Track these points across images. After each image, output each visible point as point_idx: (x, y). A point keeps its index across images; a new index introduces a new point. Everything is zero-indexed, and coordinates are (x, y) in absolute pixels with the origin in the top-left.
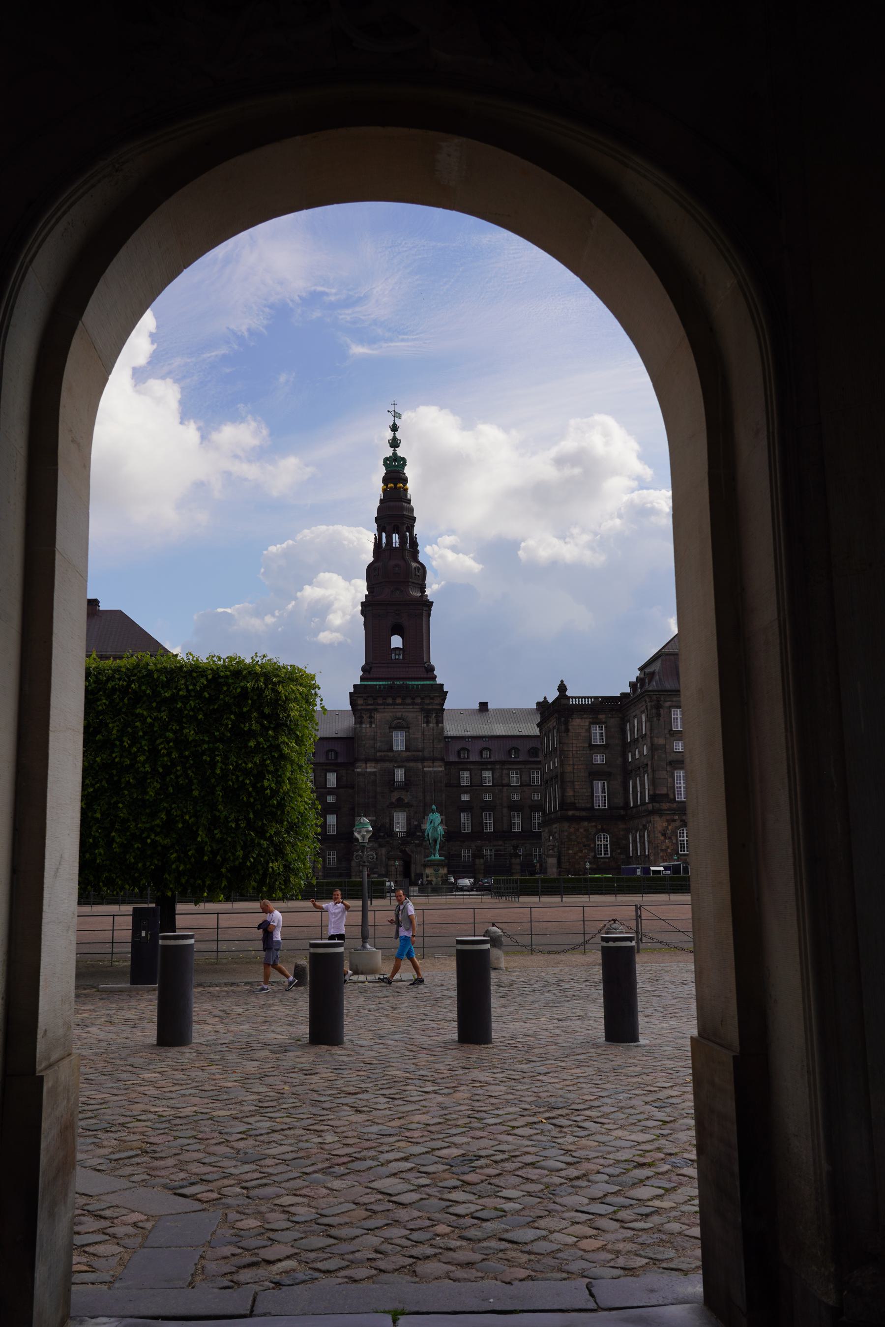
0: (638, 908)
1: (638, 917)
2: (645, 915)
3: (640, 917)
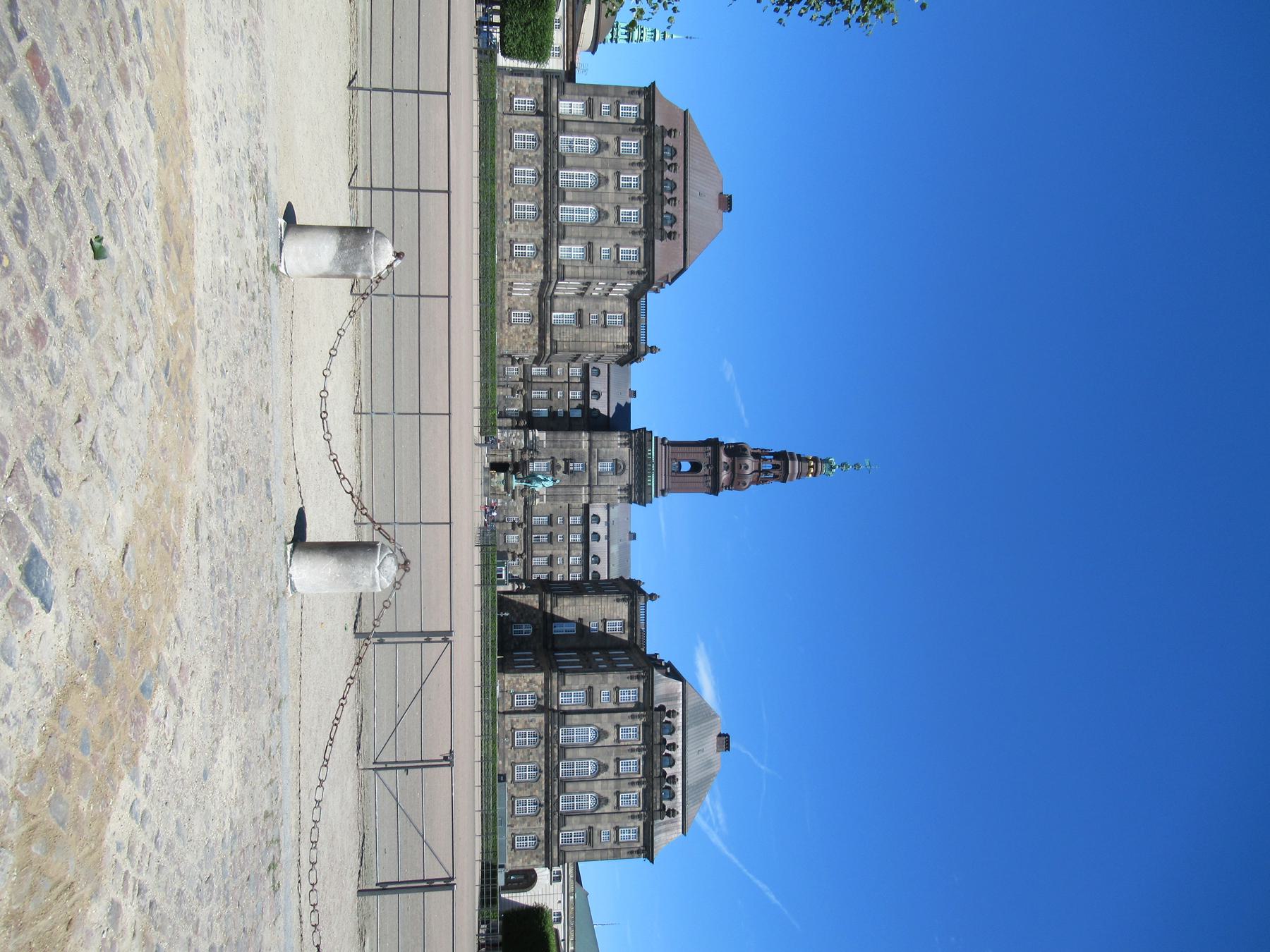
0: (446, 636)
1: (428, 636)
2: (434, 649)
3: (428, 641)
